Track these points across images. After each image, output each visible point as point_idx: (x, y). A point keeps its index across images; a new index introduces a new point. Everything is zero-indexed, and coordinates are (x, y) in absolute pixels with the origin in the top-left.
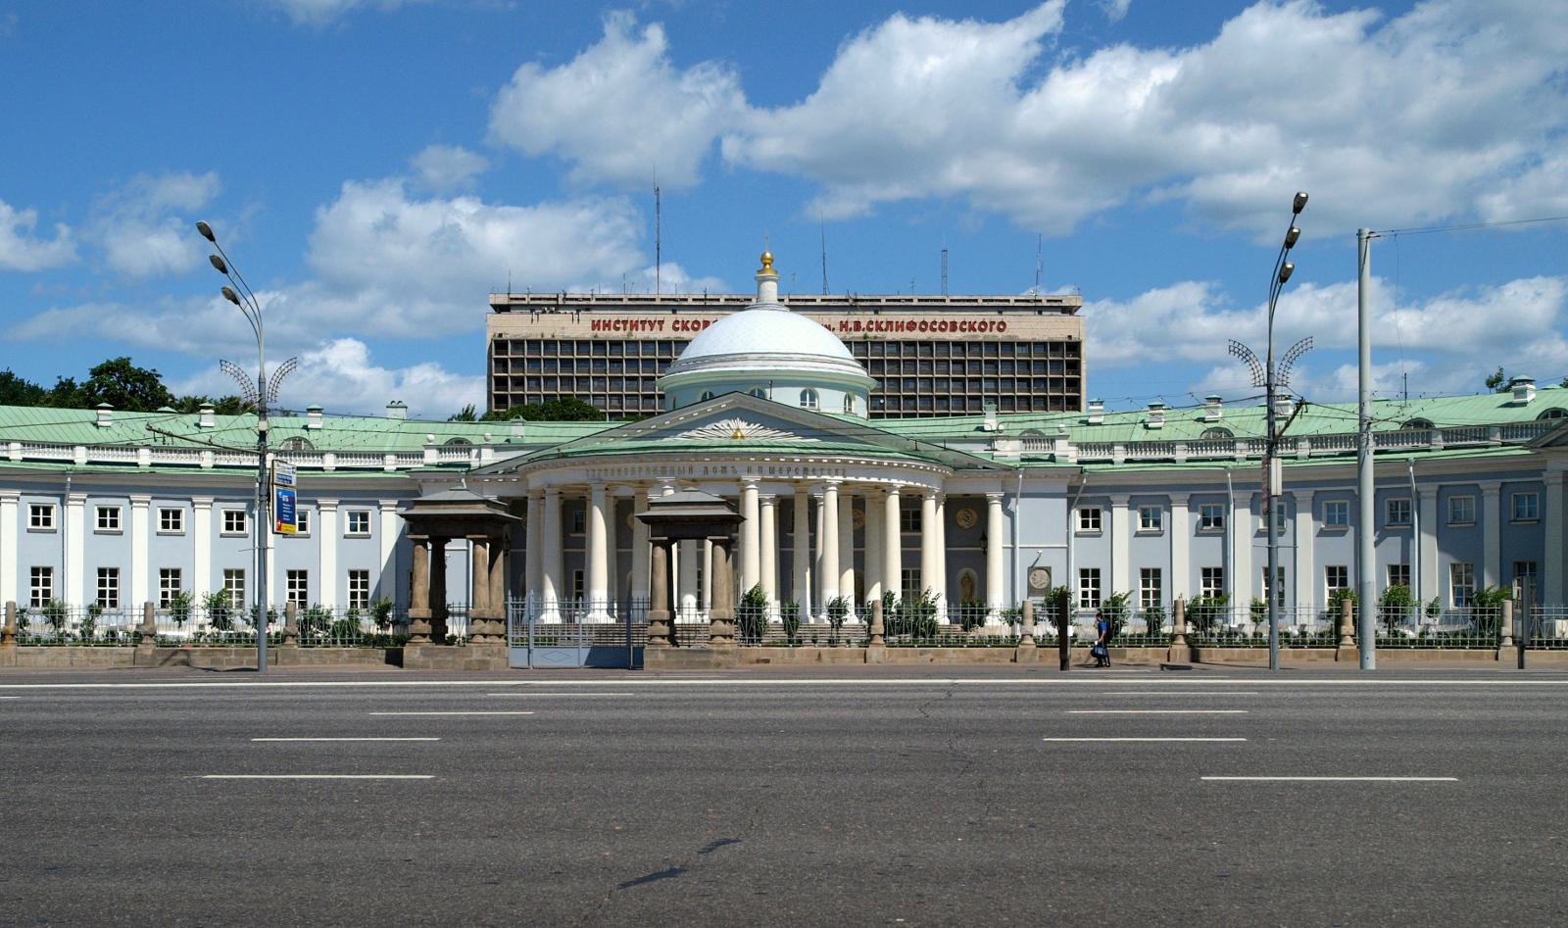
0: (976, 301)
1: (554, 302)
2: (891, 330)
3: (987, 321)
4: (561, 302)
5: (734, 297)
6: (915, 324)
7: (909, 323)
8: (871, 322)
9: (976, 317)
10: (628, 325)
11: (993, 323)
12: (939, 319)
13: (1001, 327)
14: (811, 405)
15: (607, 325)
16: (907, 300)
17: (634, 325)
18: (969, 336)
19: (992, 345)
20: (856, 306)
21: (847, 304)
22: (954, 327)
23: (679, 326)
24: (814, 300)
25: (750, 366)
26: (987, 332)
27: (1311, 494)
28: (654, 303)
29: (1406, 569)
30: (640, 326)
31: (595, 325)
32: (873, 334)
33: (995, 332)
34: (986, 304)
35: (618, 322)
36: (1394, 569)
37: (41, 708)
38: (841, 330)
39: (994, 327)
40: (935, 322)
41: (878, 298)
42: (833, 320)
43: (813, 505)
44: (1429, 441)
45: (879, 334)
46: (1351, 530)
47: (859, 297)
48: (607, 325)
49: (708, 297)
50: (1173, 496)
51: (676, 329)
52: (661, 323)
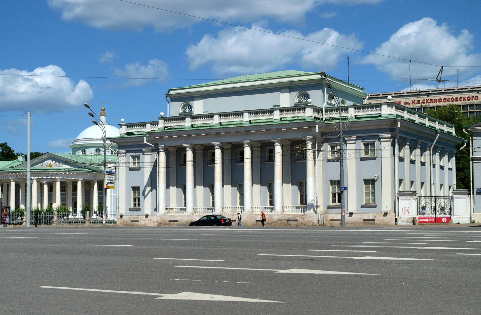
2: (432, 103)
3: (471, 96)
5: (374, 94)
6: (441, 99)
7: (439, 99)
8: (424, 100)
9: (466, 95)
11: (473, 97)
12: (451, 97)
13: (476, 98)
14: (99, 153)
18: (463, 103)
19: (471, 106)
20: (419, 94)
22: (457, 99)
26: (471, 101)
32: (425, 104)
33: (474, 100)
34: (472, 90)
37: (243, 245)
38: (413, 104)
39: (474, 98)
40: (449, 98)
42: (409, 100)
45: (427, 104)
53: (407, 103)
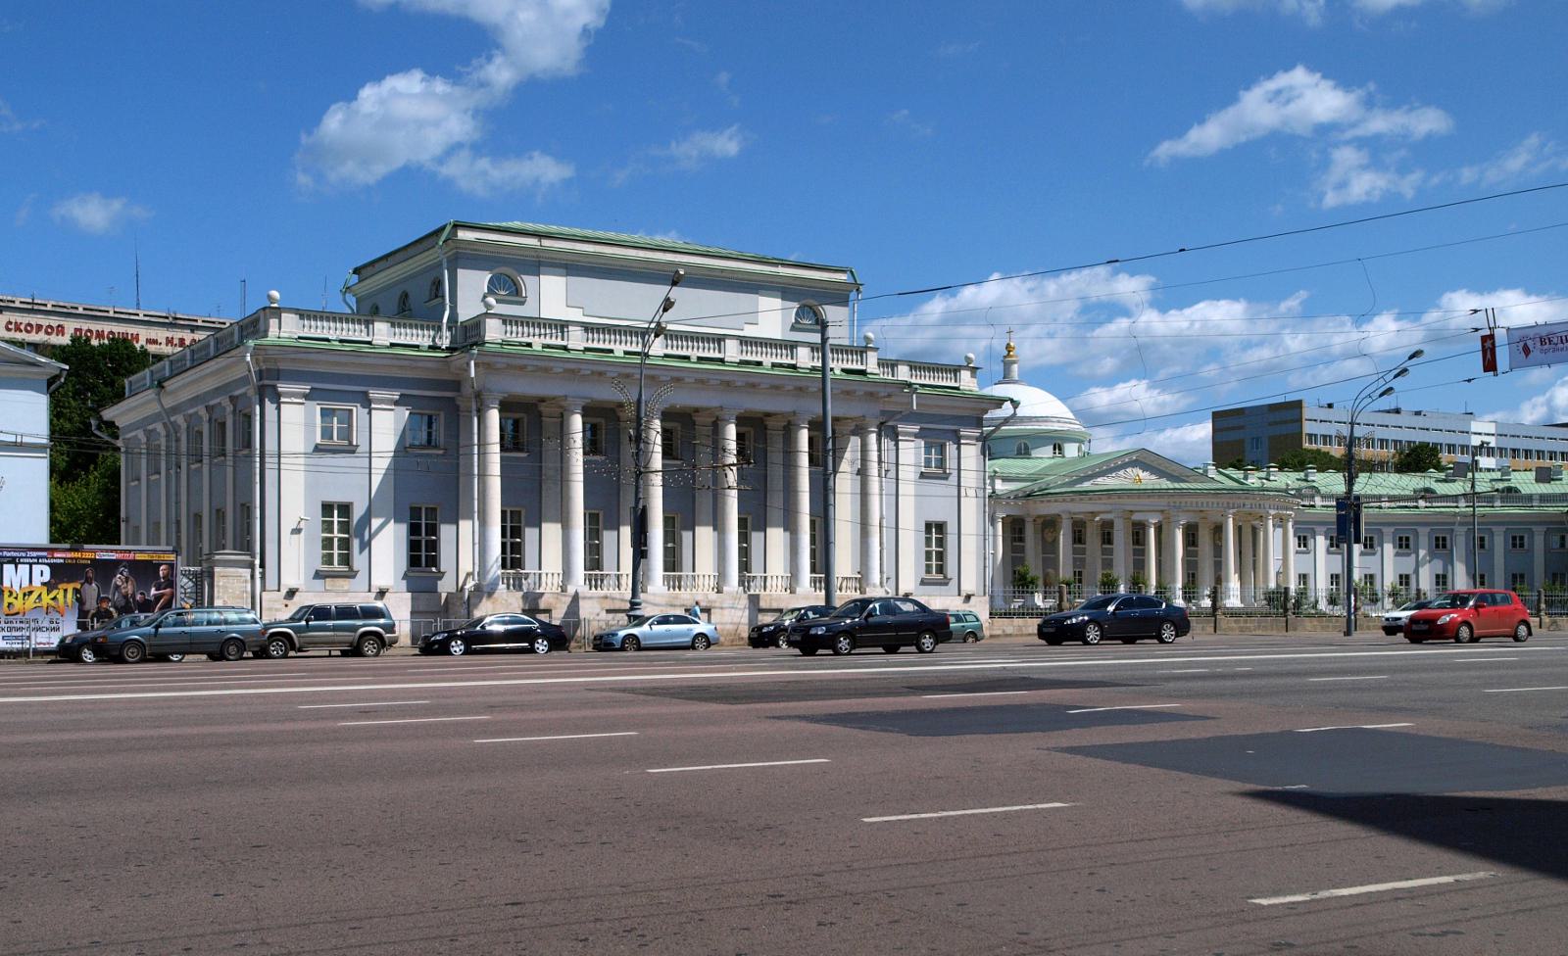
0: (196, 321)
5: (61, 304)
16: (220, 323)
21: (167, 321)
23: (12, 326)
24: (196, 321)
25: (1056, 426)
27: (1393, 530)
29: (1445, 577)
36: (1437, 576)
41: (106, 309)
42: (159, 335)
43: (1218, 530)
44: (1457, 502)
46: (1413, 556)
47: (178, 316)
49: (36, 301)
50: (1318, 529)
51: (9, 330)
53: (155, 342)
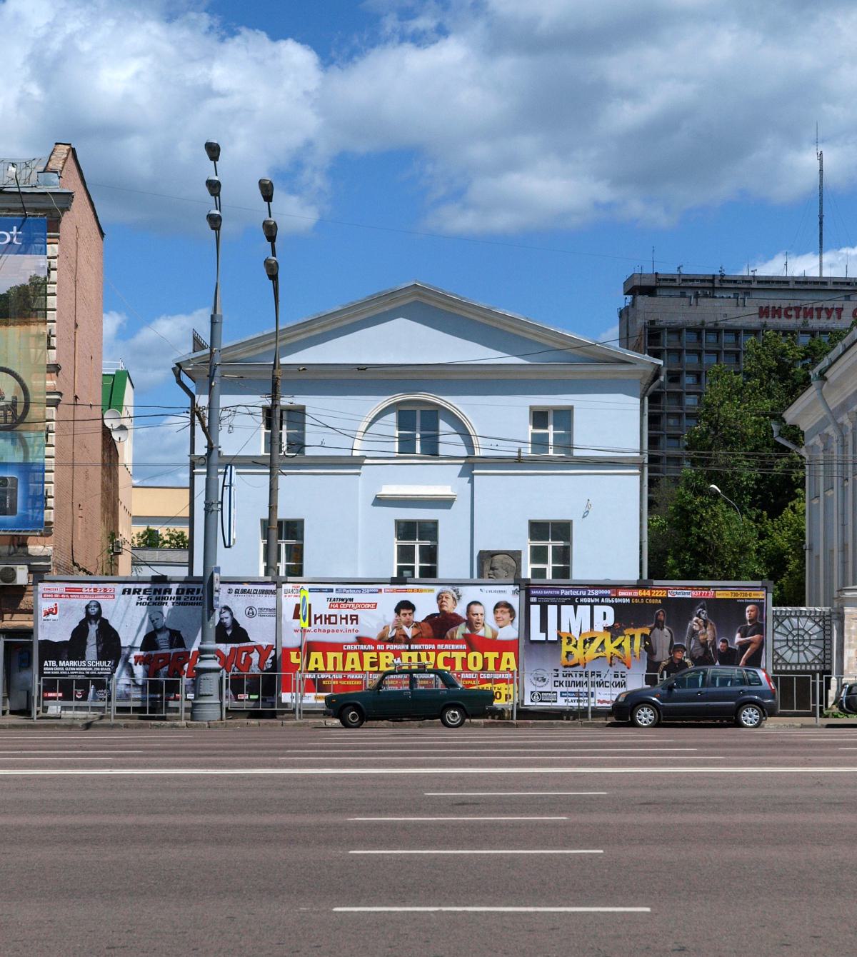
1: (710, 285)
4: (717, 285)
10: (801, 313)
15: (777, 312)
17: (809, 313)
28: (826, 287)
30: (815, 313)
31: (763, 312)
35: (790, 309)
48: (777, 312)
52: (840, 310)
